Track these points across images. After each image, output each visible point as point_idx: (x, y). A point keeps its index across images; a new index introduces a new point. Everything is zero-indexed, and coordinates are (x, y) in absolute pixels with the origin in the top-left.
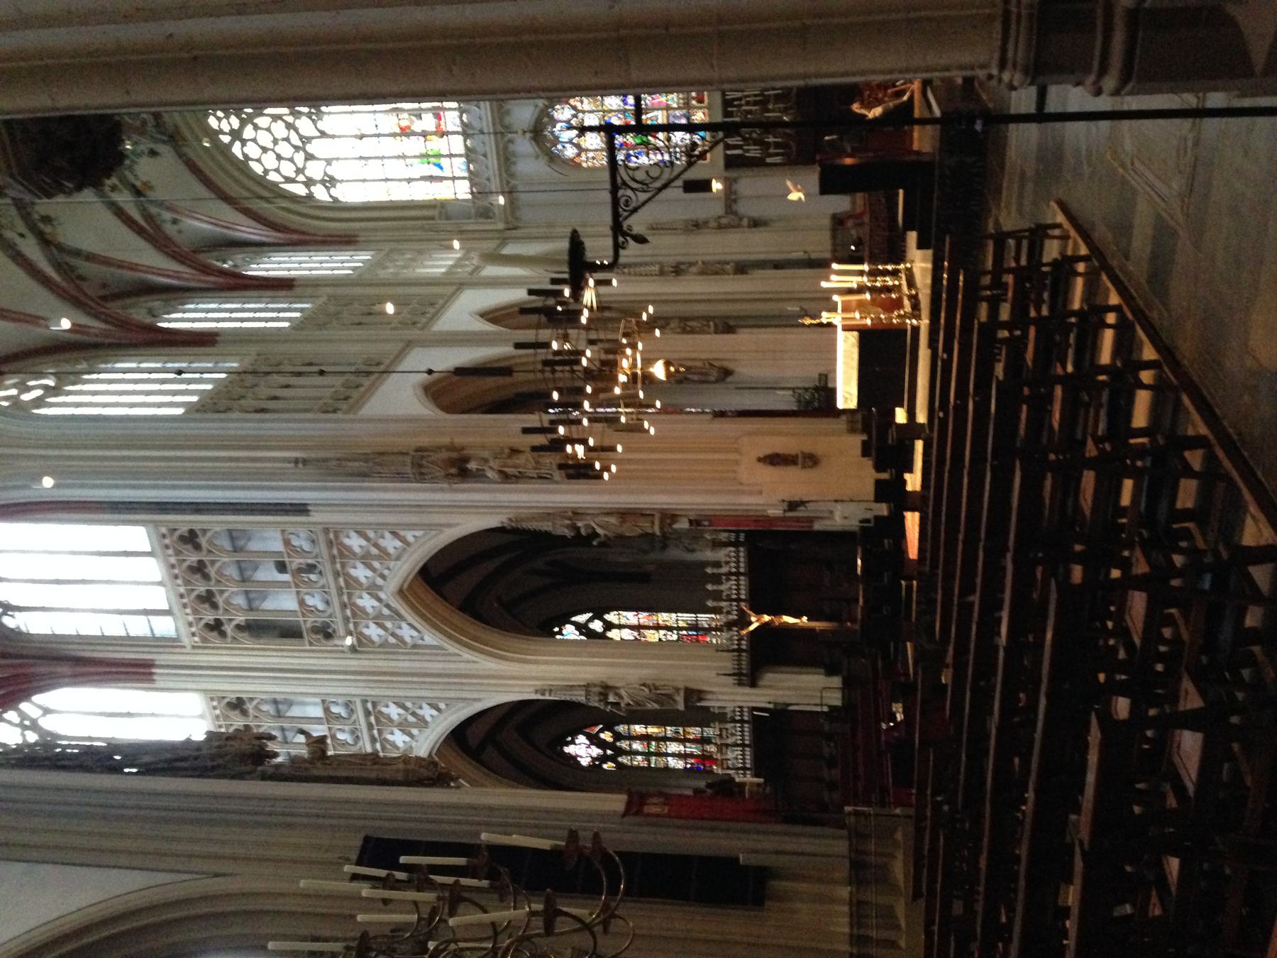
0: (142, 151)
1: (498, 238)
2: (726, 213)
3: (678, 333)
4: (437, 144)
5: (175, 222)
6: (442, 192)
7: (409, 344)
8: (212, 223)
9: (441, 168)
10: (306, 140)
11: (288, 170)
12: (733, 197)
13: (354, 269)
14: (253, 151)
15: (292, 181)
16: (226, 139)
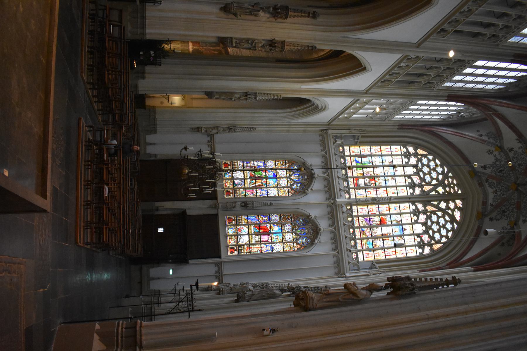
0: (490, 168)
1: (332, 125)
2: (213, 135)
3: (257, 39)
4: (357, 172)
5: (481, 135)
6: (356, 150)
7: (418, 45)
8: (465, 135)
9: (356, 161)
10: (417, 174)
11: (425, 161)
12: (210, 143)
13: (408, 109)
14: (439, 169)
15: (423, 155)
16: (450, 174)
